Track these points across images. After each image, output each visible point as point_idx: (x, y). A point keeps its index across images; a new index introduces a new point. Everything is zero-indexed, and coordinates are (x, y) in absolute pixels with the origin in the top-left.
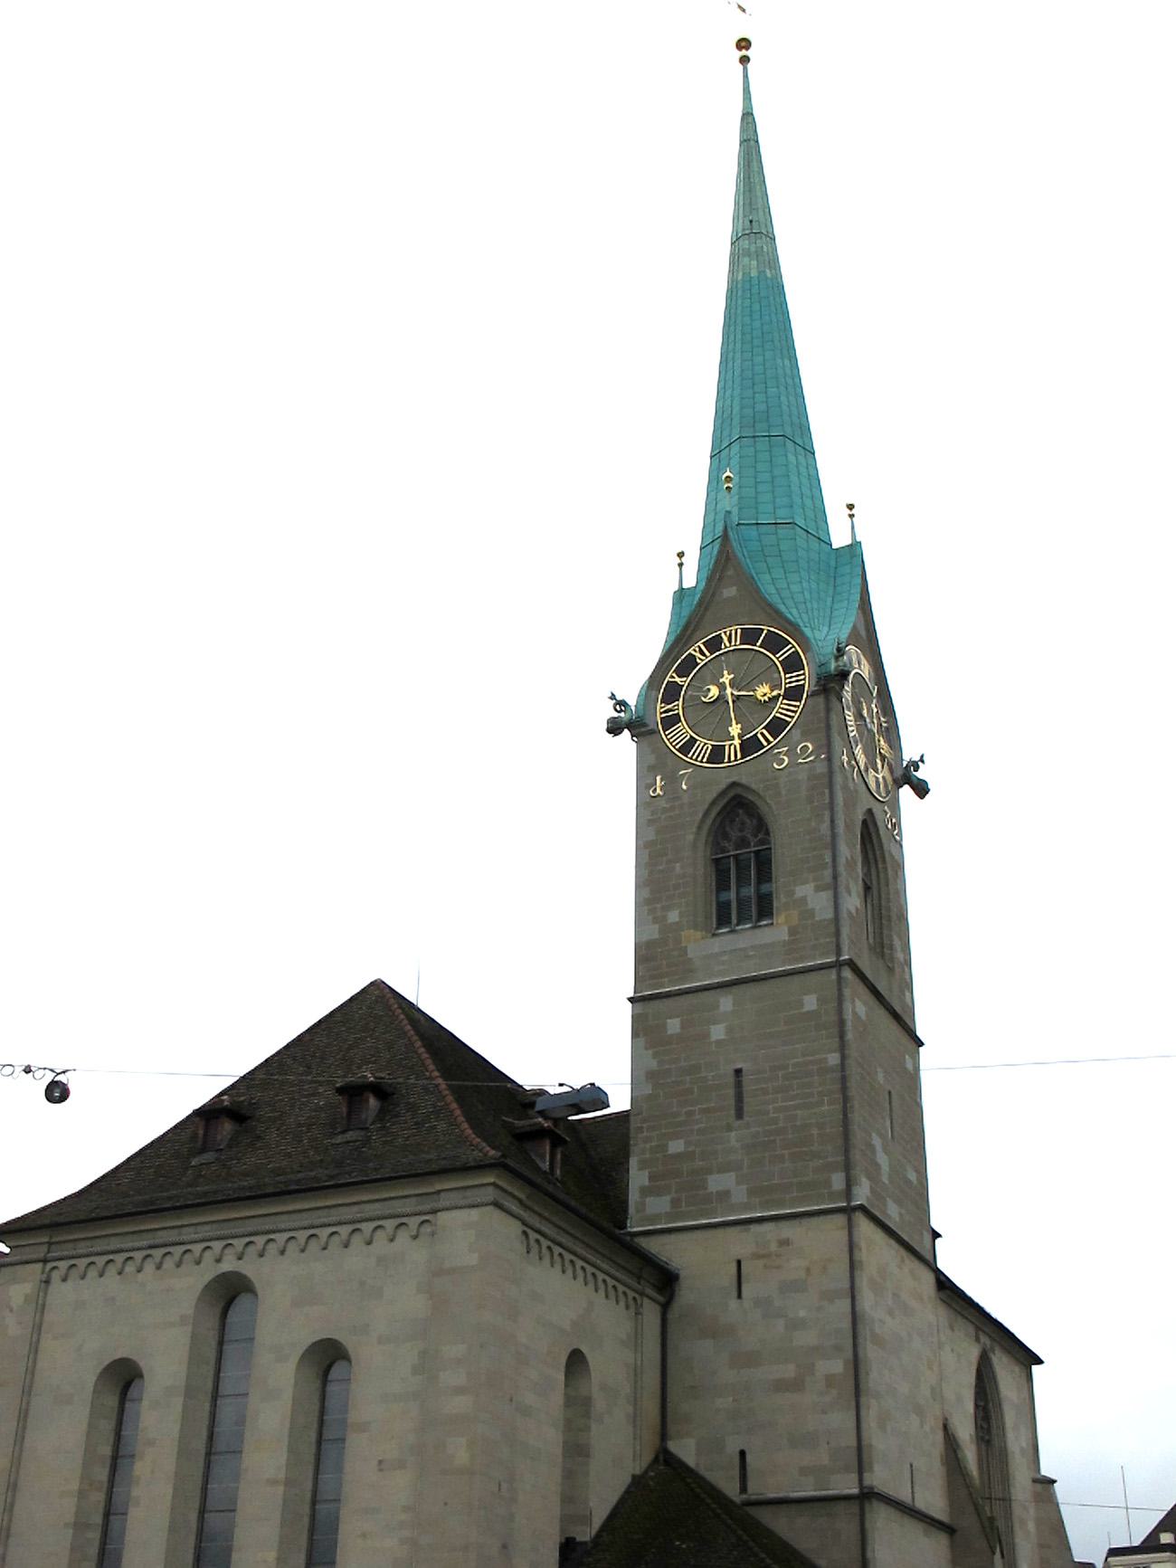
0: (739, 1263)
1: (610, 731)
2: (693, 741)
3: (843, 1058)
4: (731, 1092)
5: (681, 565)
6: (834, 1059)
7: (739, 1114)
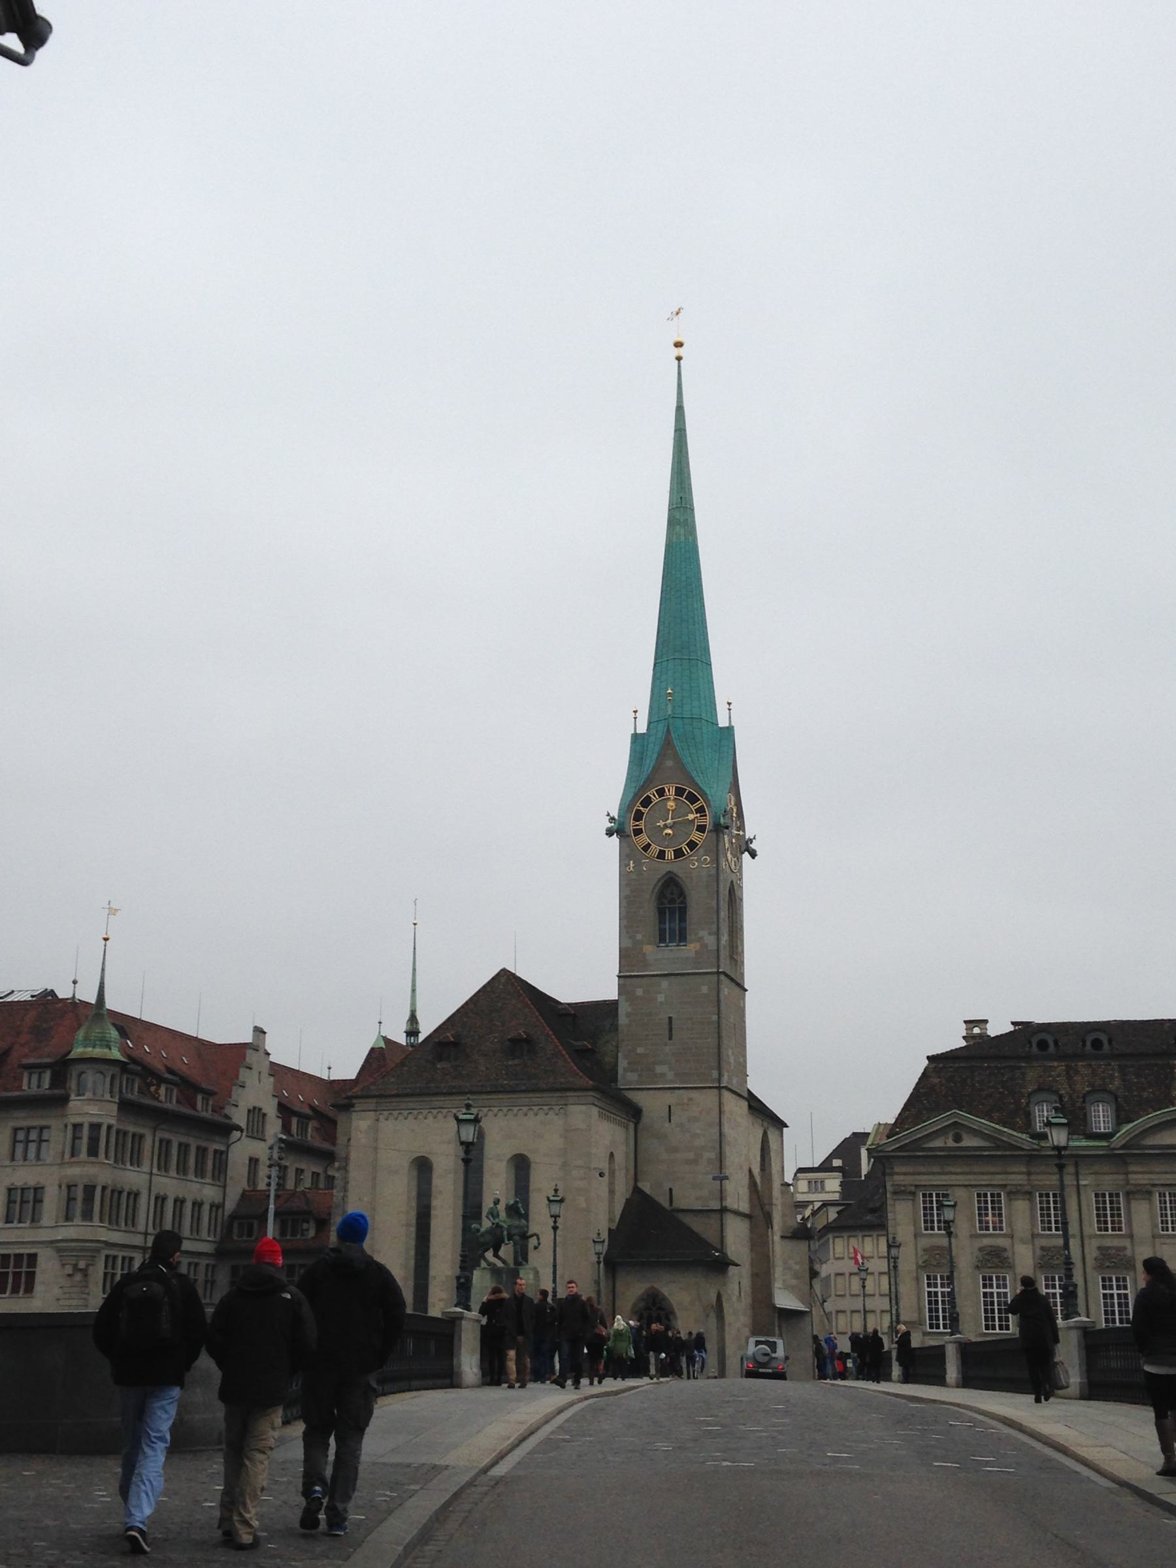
0: (670, 1107)
1: (607, 834)
2: (649, 845)
3: (719, 1017)
4: (667, 1027)
5: (635, 718)
6: (715, 1018)
7: (670, 1038)
